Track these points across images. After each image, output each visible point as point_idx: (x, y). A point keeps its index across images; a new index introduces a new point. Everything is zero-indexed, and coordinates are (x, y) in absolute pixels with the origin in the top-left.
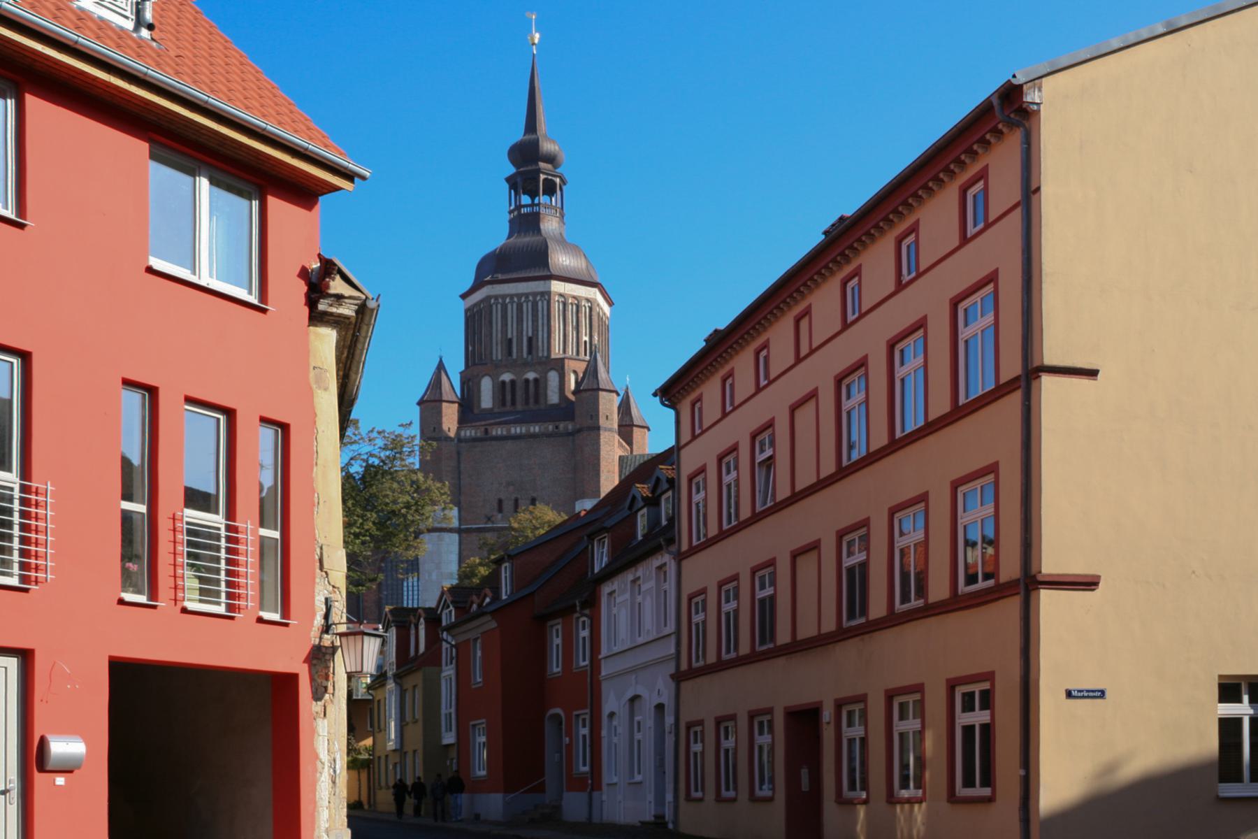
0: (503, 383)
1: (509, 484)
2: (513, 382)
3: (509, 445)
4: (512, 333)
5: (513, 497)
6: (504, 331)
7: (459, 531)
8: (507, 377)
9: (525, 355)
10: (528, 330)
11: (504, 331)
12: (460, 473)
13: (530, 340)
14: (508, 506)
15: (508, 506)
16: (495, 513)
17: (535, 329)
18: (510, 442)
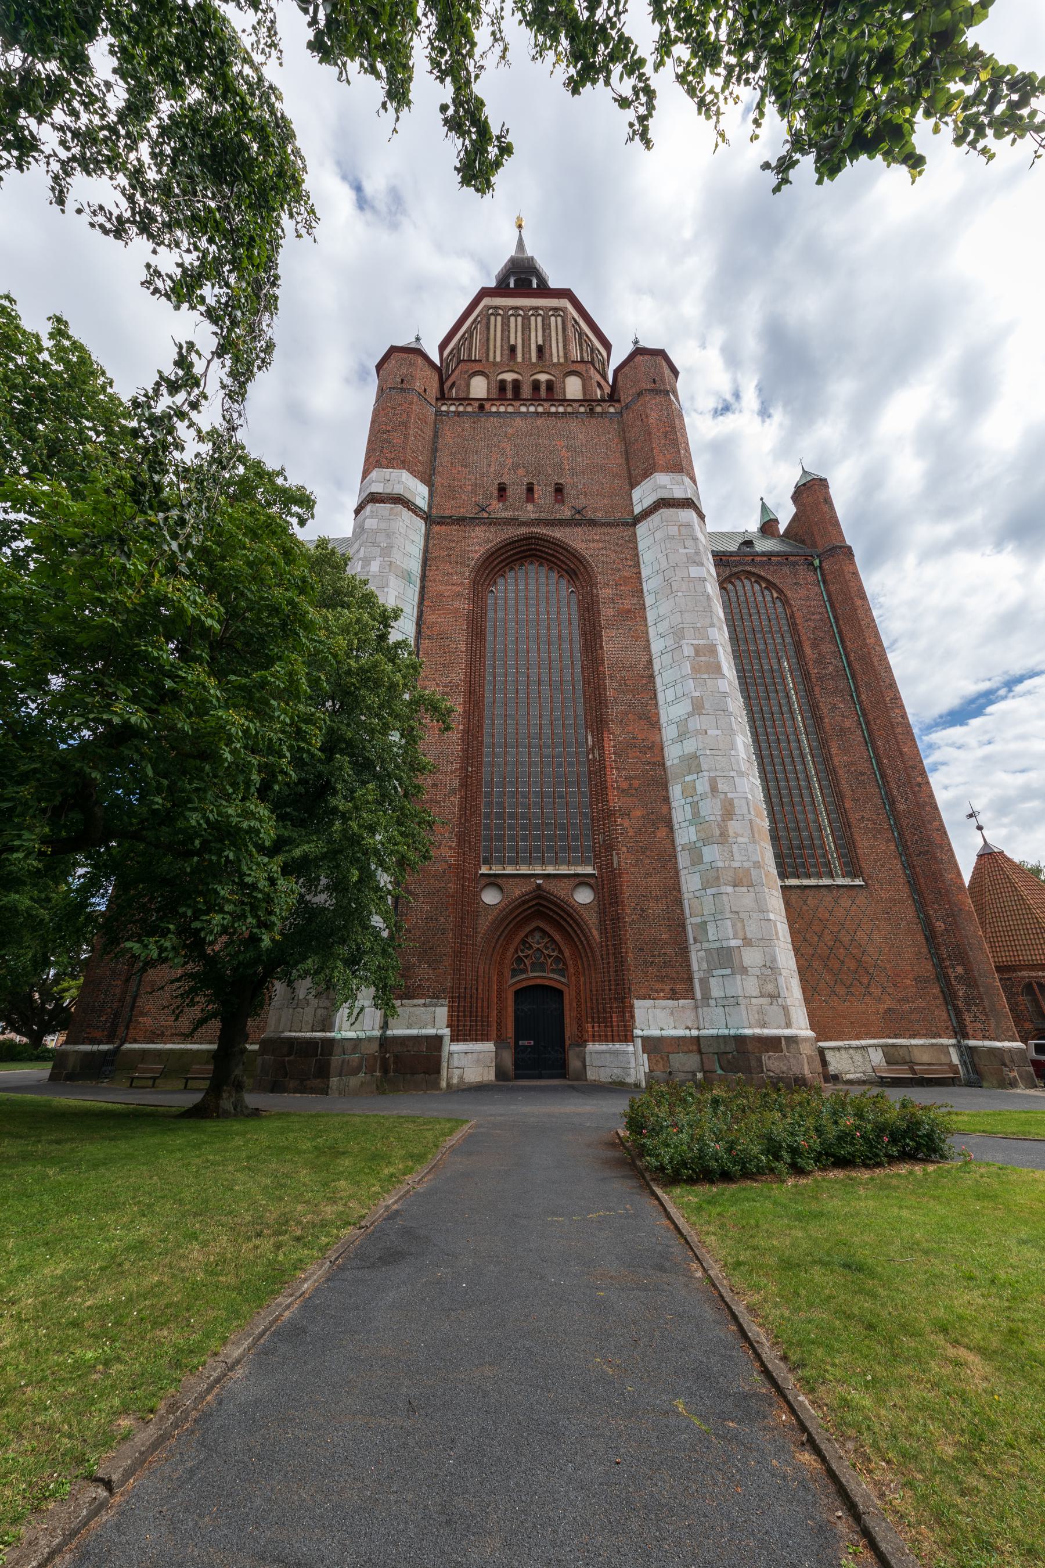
0: (503, 382)
1: (516, 466)
2: (516, 384)
3: (518, 422)
4: (516, 338)
5: (526, 480)
6: (506, 336)
7: (428, 519)
8: (509, 377)
9: (534, 360)
10: (536, 337)
11: (506, 336)
12: (435, 450)
13: (540, 349)
14: (517, 493)
15: (517, 493)
16: (494, 502)
17: (547, 337)
18: (518, 419)
